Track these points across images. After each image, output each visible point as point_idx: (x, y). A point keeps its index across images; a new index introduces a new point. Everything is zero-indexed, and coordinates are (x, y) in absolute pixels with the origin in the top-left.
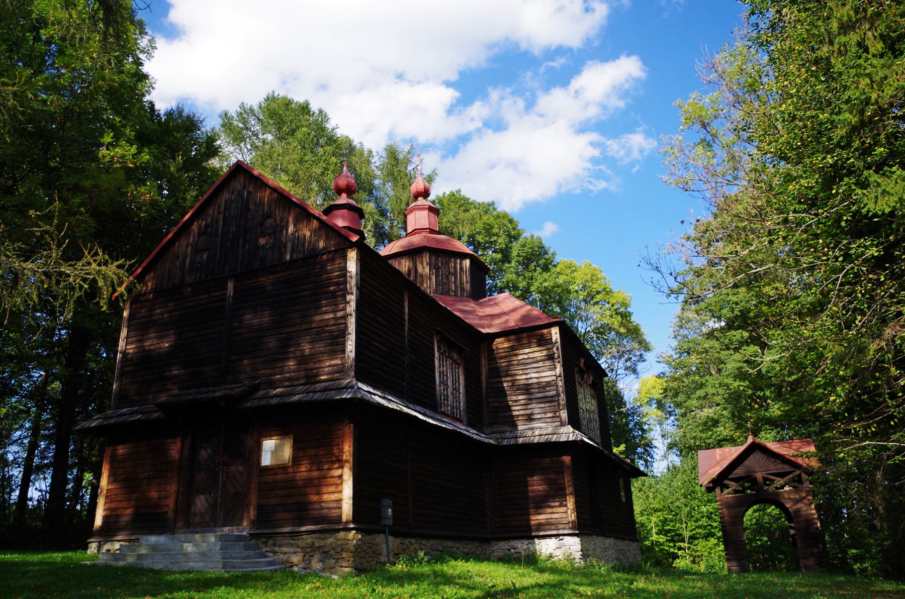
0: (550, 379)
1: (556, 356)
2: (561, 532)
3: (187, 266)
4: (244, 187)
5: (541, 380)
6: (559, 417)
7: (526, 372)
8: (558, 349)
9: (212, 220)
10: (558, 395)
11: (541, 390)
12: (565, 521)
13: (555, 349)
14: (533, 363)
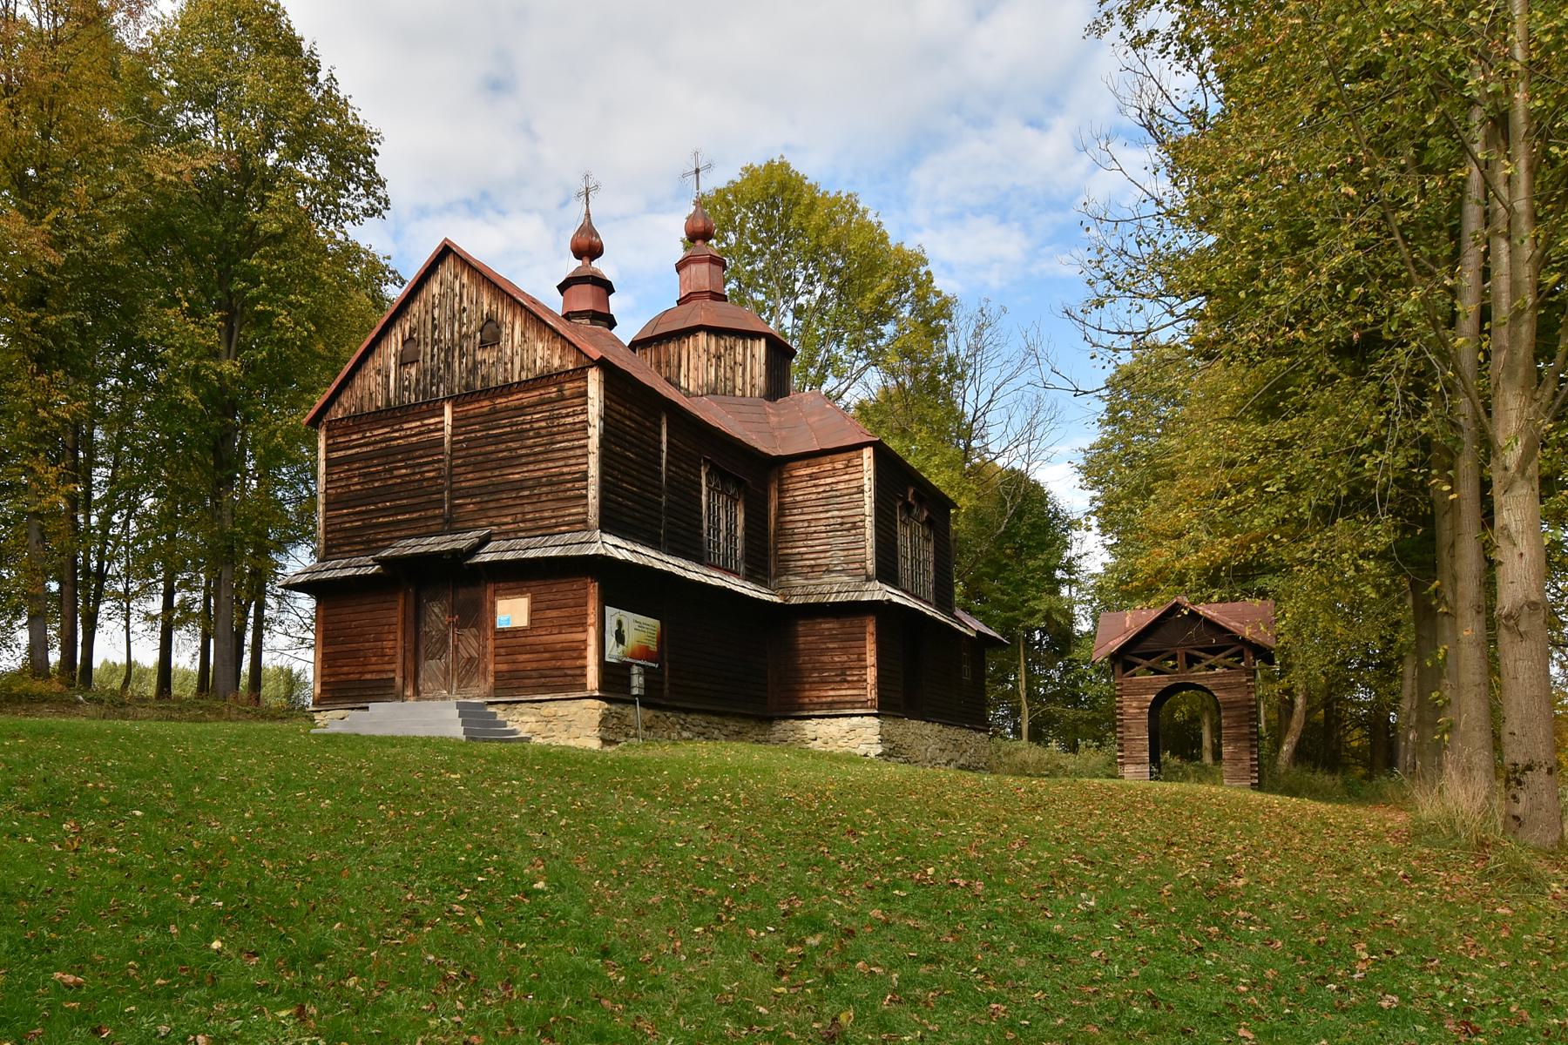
4: (456, 277)
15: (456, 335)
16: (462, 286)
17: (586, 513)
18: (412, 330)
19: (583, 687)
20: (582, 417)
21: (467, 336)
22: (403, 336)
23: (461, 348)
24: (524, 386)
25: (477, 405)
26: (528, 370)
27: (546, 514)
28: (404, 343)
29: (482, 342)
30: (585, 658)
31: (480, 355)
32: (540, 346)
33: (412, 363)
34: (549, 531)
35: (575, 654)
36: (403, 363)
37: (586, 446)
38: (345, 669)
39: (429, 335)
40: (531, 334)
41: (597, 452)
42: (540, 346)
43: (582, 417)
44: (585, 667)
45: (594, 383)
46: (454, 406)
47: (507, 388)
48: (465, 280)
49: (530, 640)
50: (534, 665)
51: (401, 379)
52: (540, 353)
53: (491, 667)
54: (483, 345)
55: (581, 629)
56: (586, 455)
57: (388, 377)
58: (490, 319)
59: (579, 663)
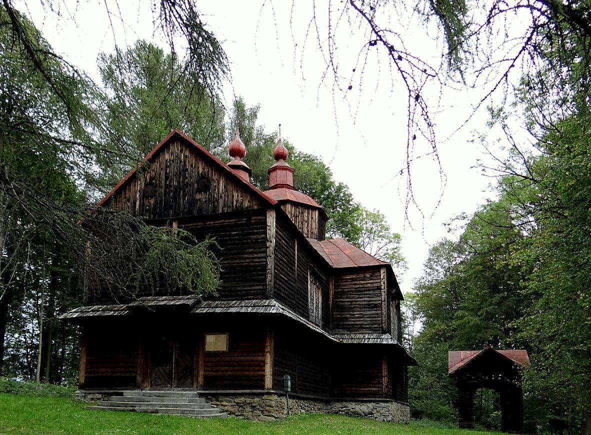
0: (377, 302)
1: (383, 287)
2: (378, 399)
3: (137, 207)
4: (181, 151)
5: (371, 303)
6: (382, 327)
7: (361, 296)
8: (384, 283)
9: (155, 174)
10: (382, 314)
11: (371, 309)
12: (380, 393)
13: (382, 283)
14: (366, 291)
15: (182, 184)
16: (186, 157)
17: (265, 290)
18: (152, 178)
19: (263, 387)
20: (262, 236)
21: (187, 185)
22: (146, 181)
23: (184, 191)
24: (225, 216)
25: (194, 224)
26: (229, 207)
27: (239, 289)
28: (146, 185)
29: (198, 188)
30: (264, 370)
31: (198, 196)
32: (235, 194)
33: (152, 197)
34: (241, 297)
35: (258, 368)
36: (145, 196)
37: (266, 252)
38: (102, 370)
39: (163, 182)
40: (230, 188)
41: (273, 256)
42: (235, 194)
43: (262, 236)
44: (264, 376)
45: (271, 219)
46: (179, 223)
47: (215, 216)
48: (187, 153)
49: (227, 359)
50: (230, 373)
51: (144, 205)
52: (235, 198)
53: (201, 373)
54: (199, 191)
55: (261, 354)
56: (266, 257)
57: (135, 203)
58: (203, 177)
59: (260, 373)
